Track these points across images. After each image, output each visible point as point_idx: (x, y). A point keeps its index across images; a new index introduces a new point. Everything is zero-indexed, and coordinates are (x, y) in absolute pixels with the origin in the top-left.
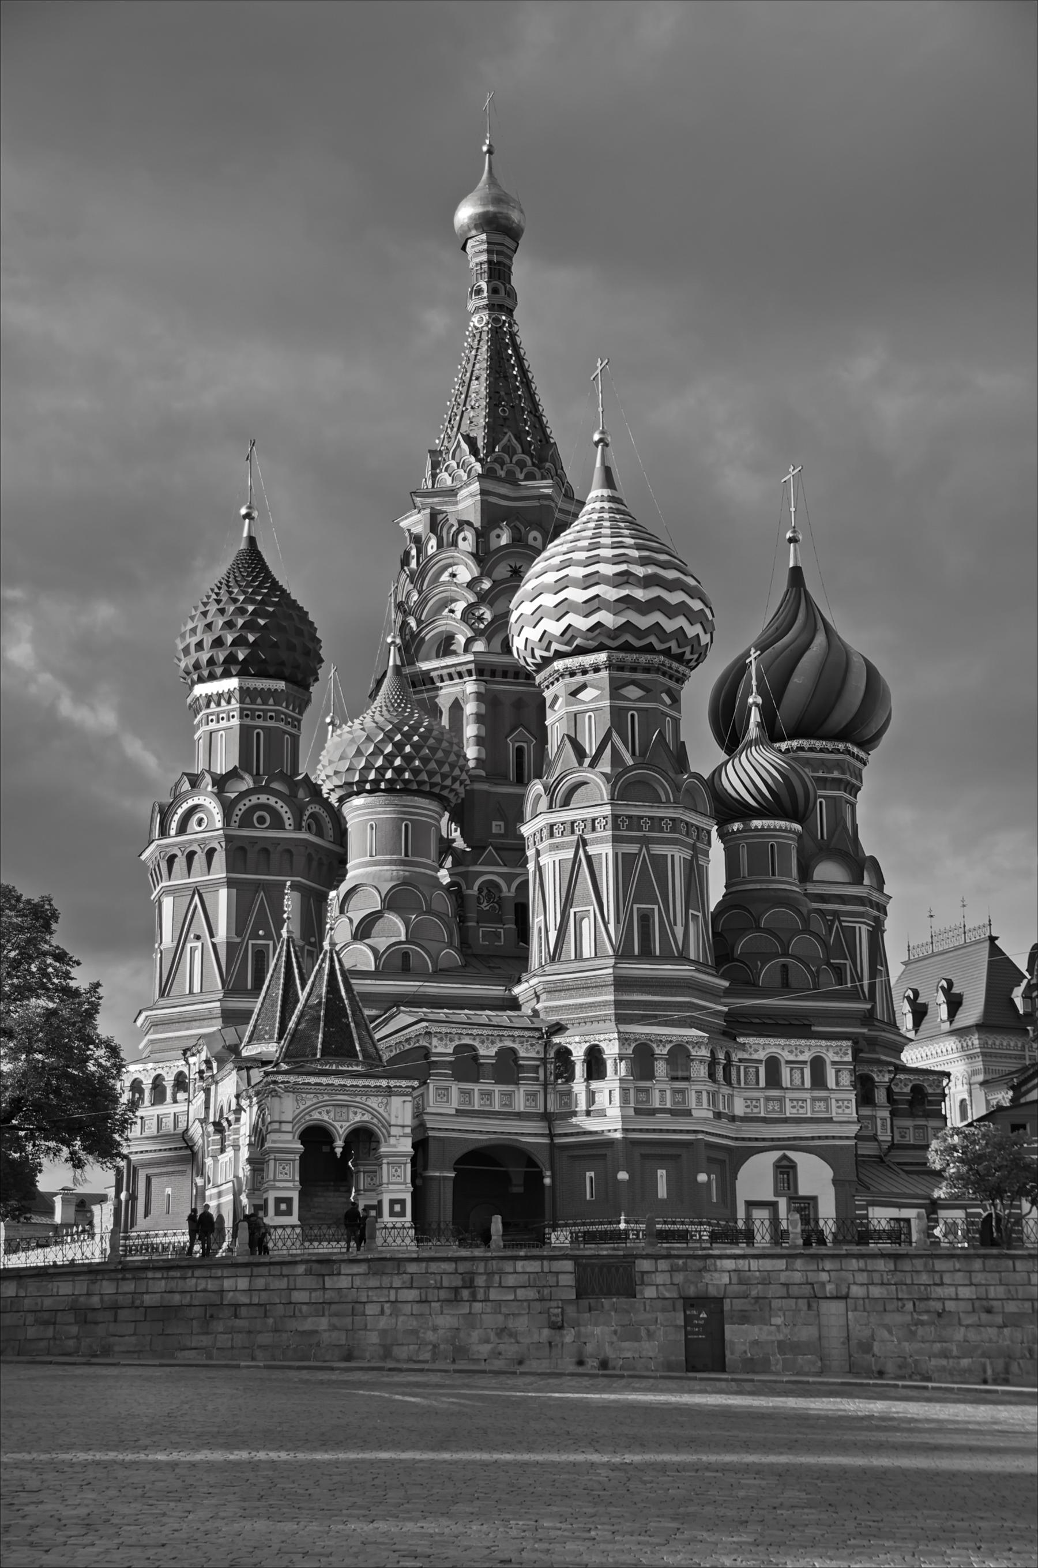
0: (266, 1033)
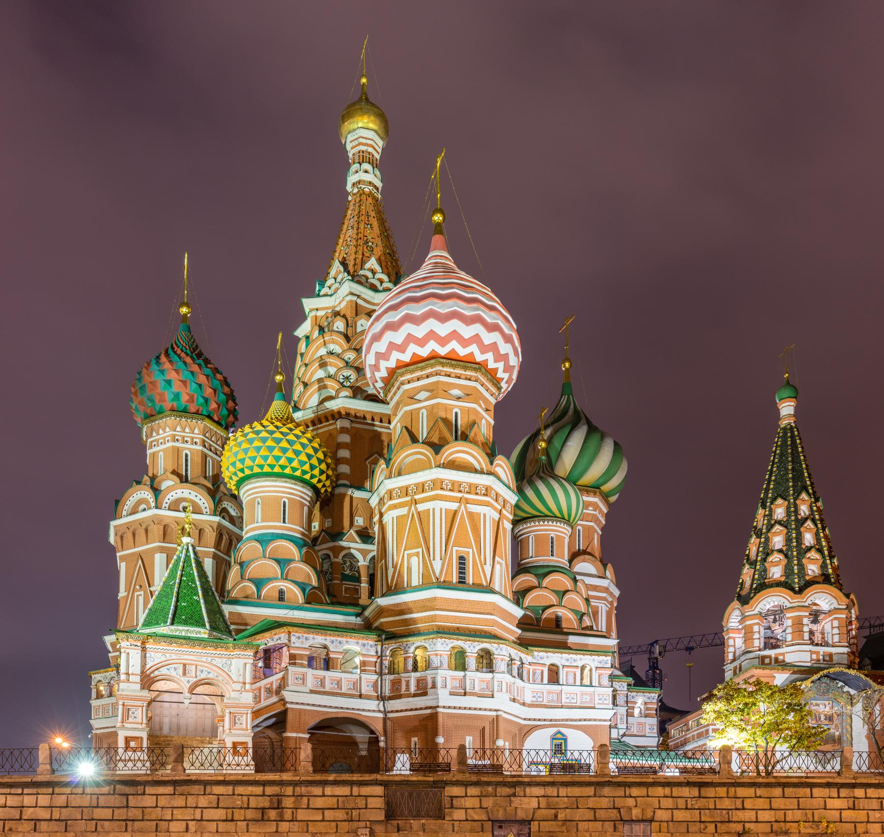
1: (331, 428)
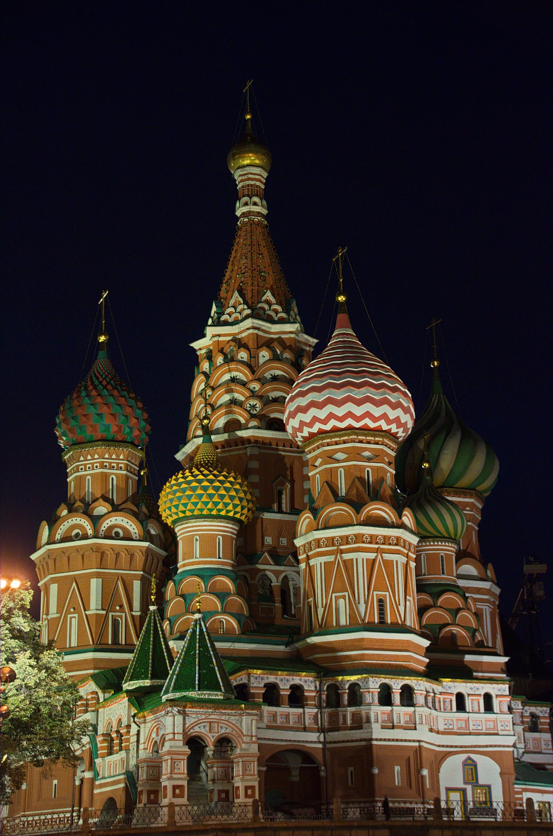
0: (142, 674)
1: (241, 452)
